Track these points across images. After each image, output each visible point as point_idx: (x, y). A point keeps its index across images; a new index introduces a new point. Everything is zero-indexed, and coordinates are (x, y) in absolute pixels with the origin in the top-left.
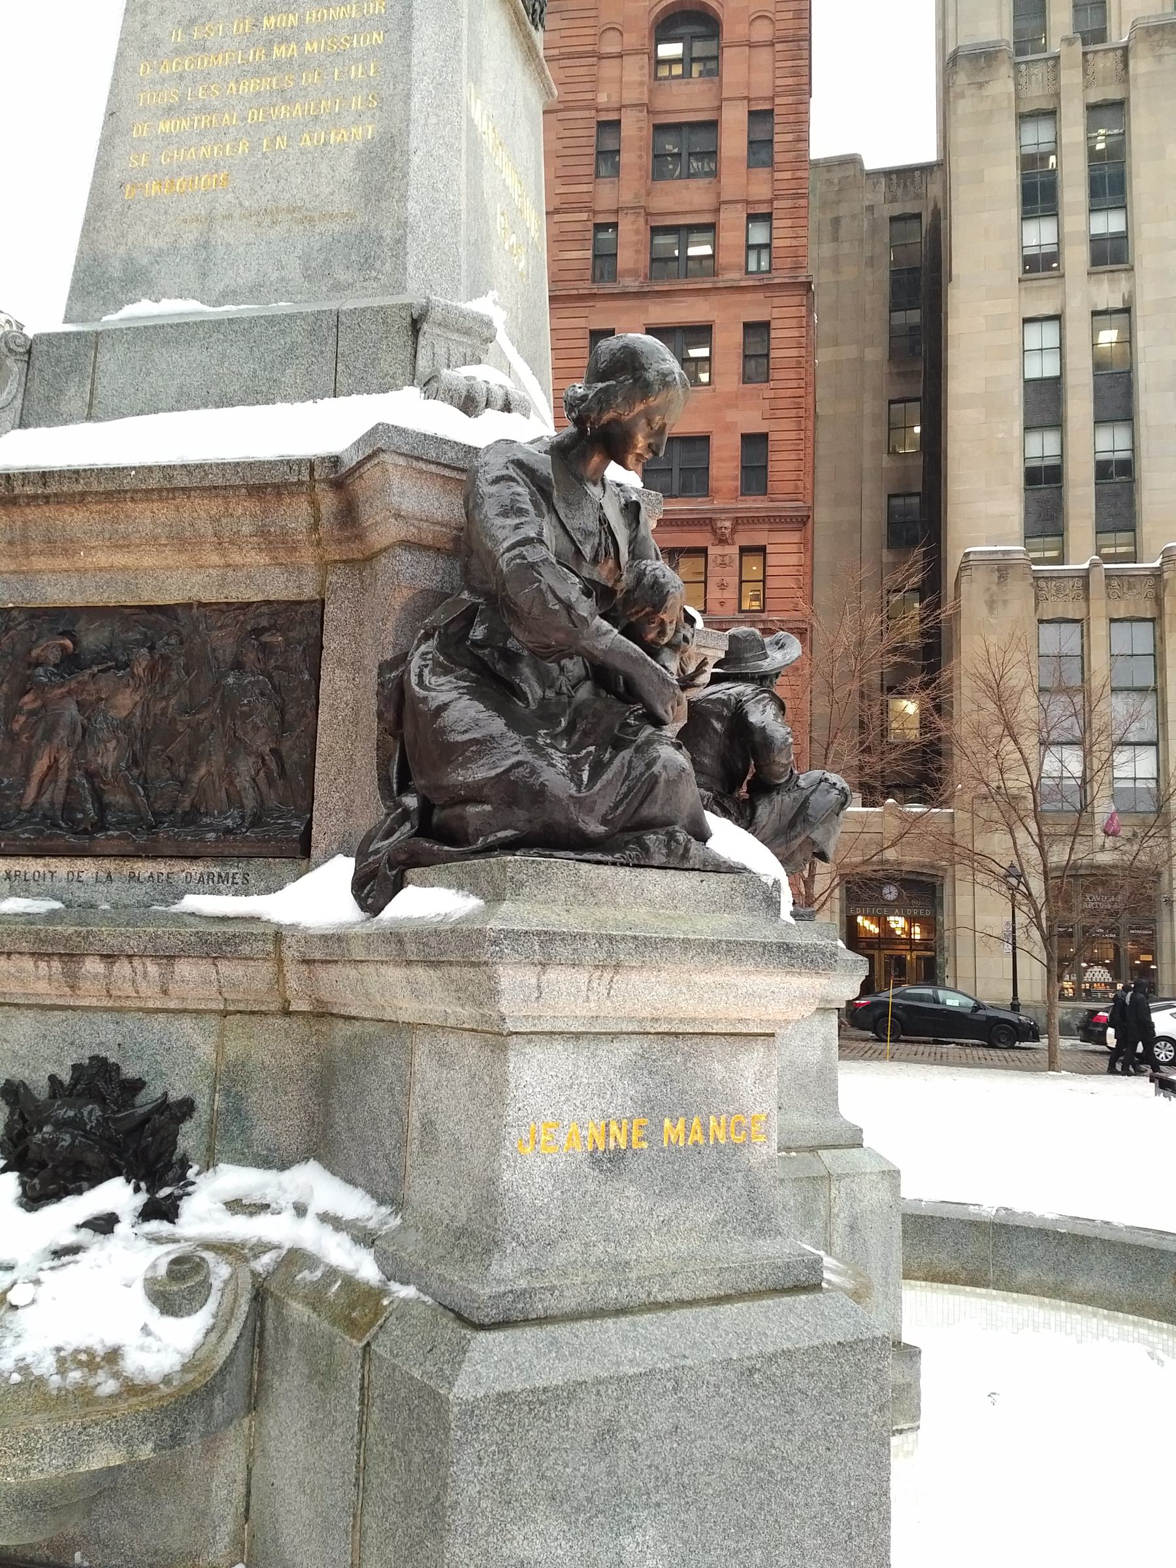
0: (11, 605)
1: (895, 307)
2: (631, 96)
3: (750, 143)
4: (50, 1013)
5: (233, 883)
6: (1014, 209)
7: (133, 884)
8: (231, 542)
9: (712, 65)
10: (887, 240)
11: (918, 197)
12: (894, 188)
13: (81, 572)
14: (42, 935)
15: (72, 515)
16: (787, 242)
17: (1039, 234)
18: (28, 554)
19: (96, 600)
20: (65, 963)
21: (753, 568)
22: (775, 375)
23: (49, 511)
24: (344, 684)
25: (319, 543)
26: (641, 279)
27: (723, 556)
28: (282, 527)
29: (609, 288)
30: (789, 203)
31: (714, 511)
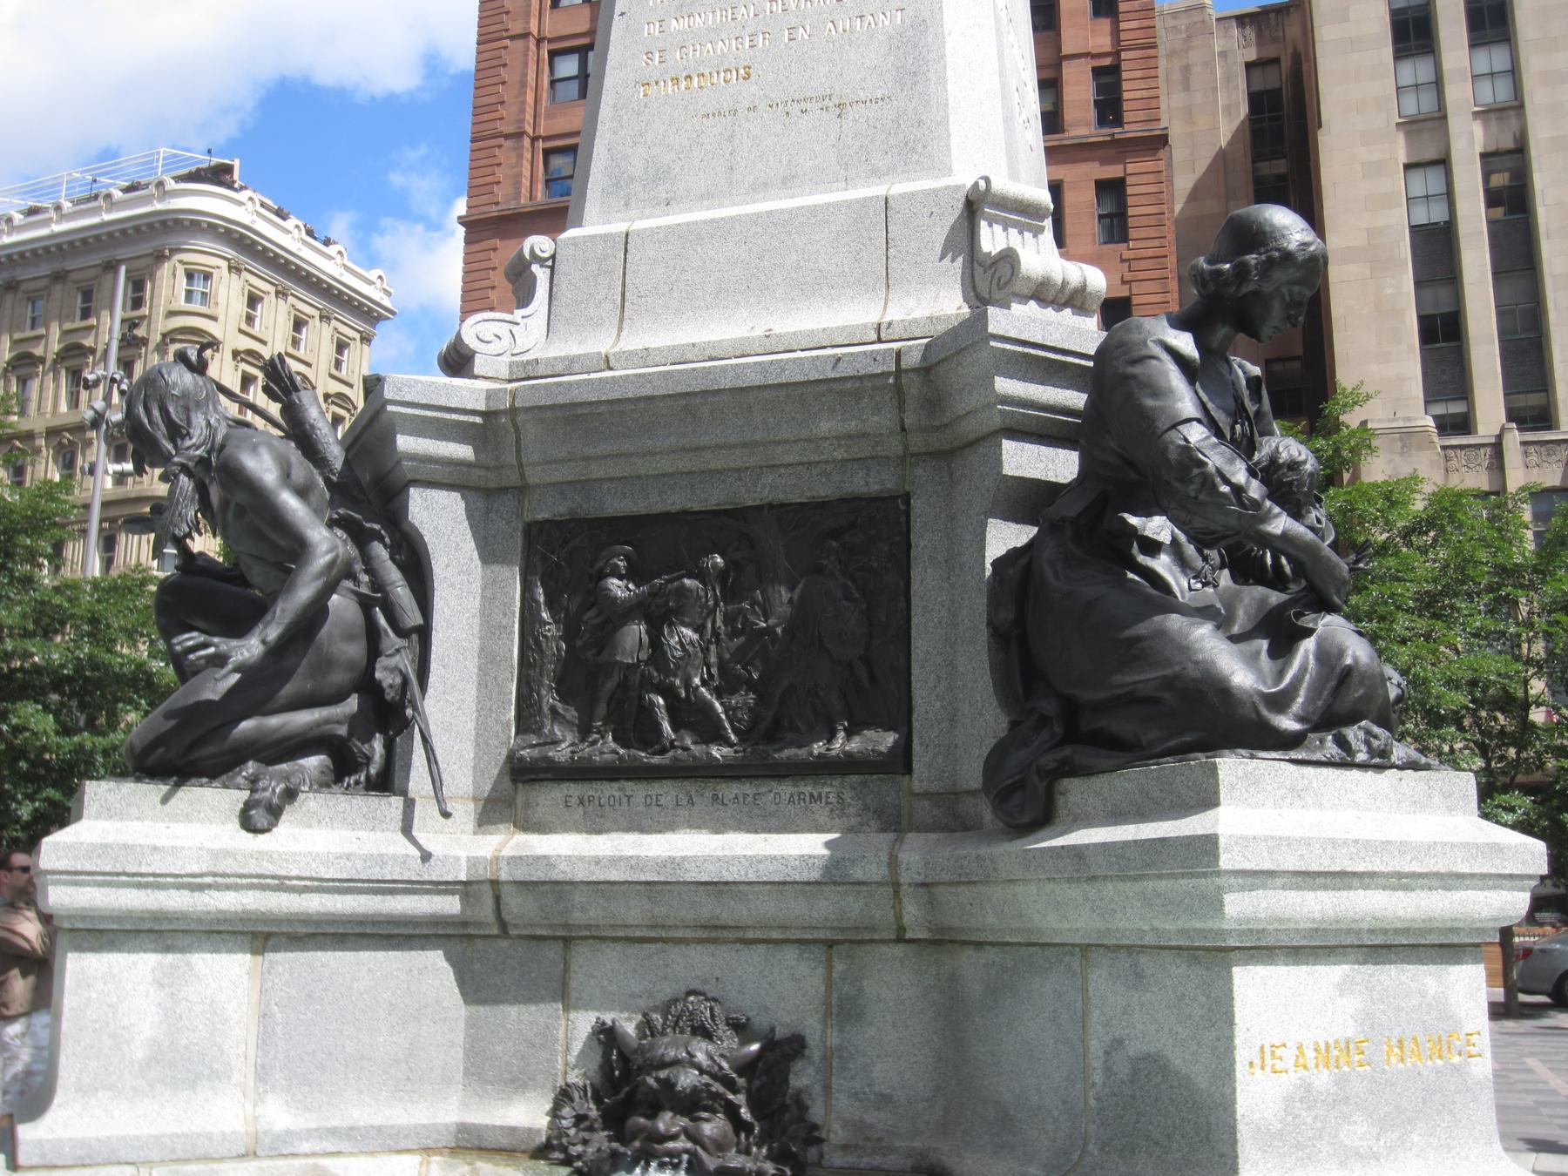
1: (1257, 157)
5: (827, 803)
6: (1388, 50)
11: (1275, 40)
22: (1133, 233)
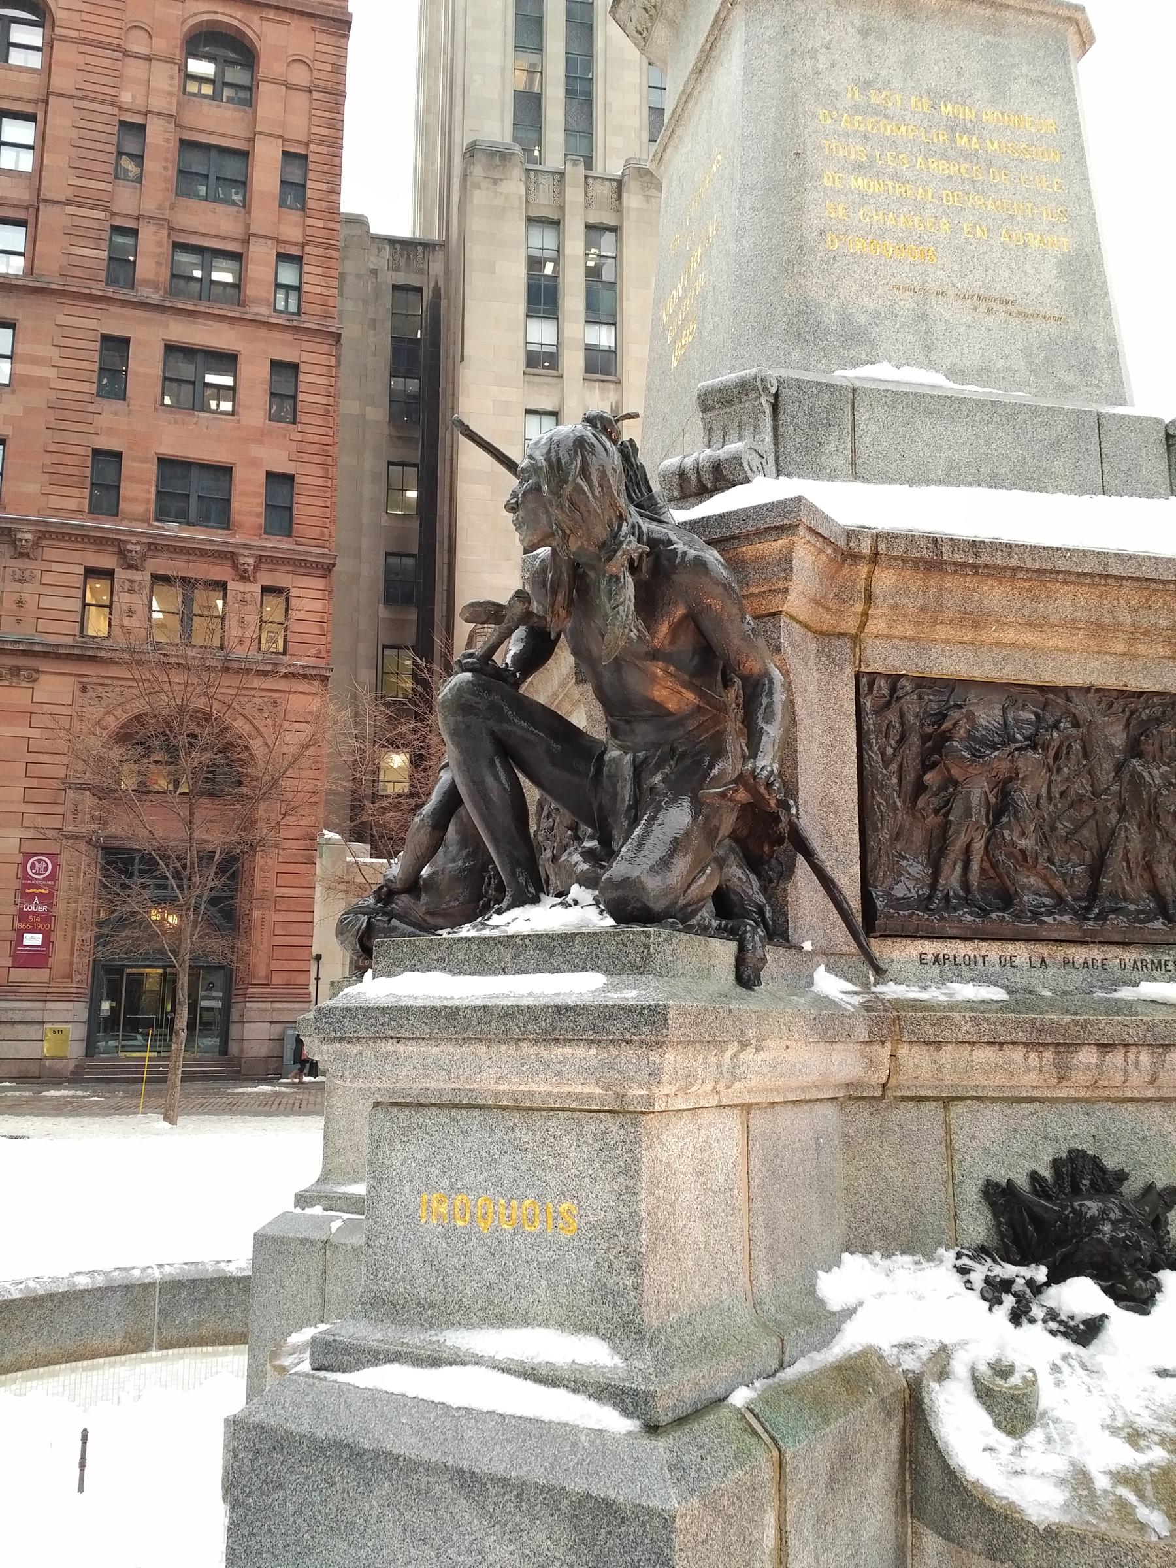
4: (1017, 1106)
6: (522, 308)
7: (1069, 969)
8: (1144, 634)
10: (389, 306)
11: (420, 271)
12: (397, 257)
14: (1038, 1024)
16: (318, 290)
17: (541, 333)
18: (935, 622)
21: (272, 608)
22: (301, 417)
23: (971, 582)
26: (162, 292)
27: (244, 593)
29: (126, 294)
31: (236, 545)
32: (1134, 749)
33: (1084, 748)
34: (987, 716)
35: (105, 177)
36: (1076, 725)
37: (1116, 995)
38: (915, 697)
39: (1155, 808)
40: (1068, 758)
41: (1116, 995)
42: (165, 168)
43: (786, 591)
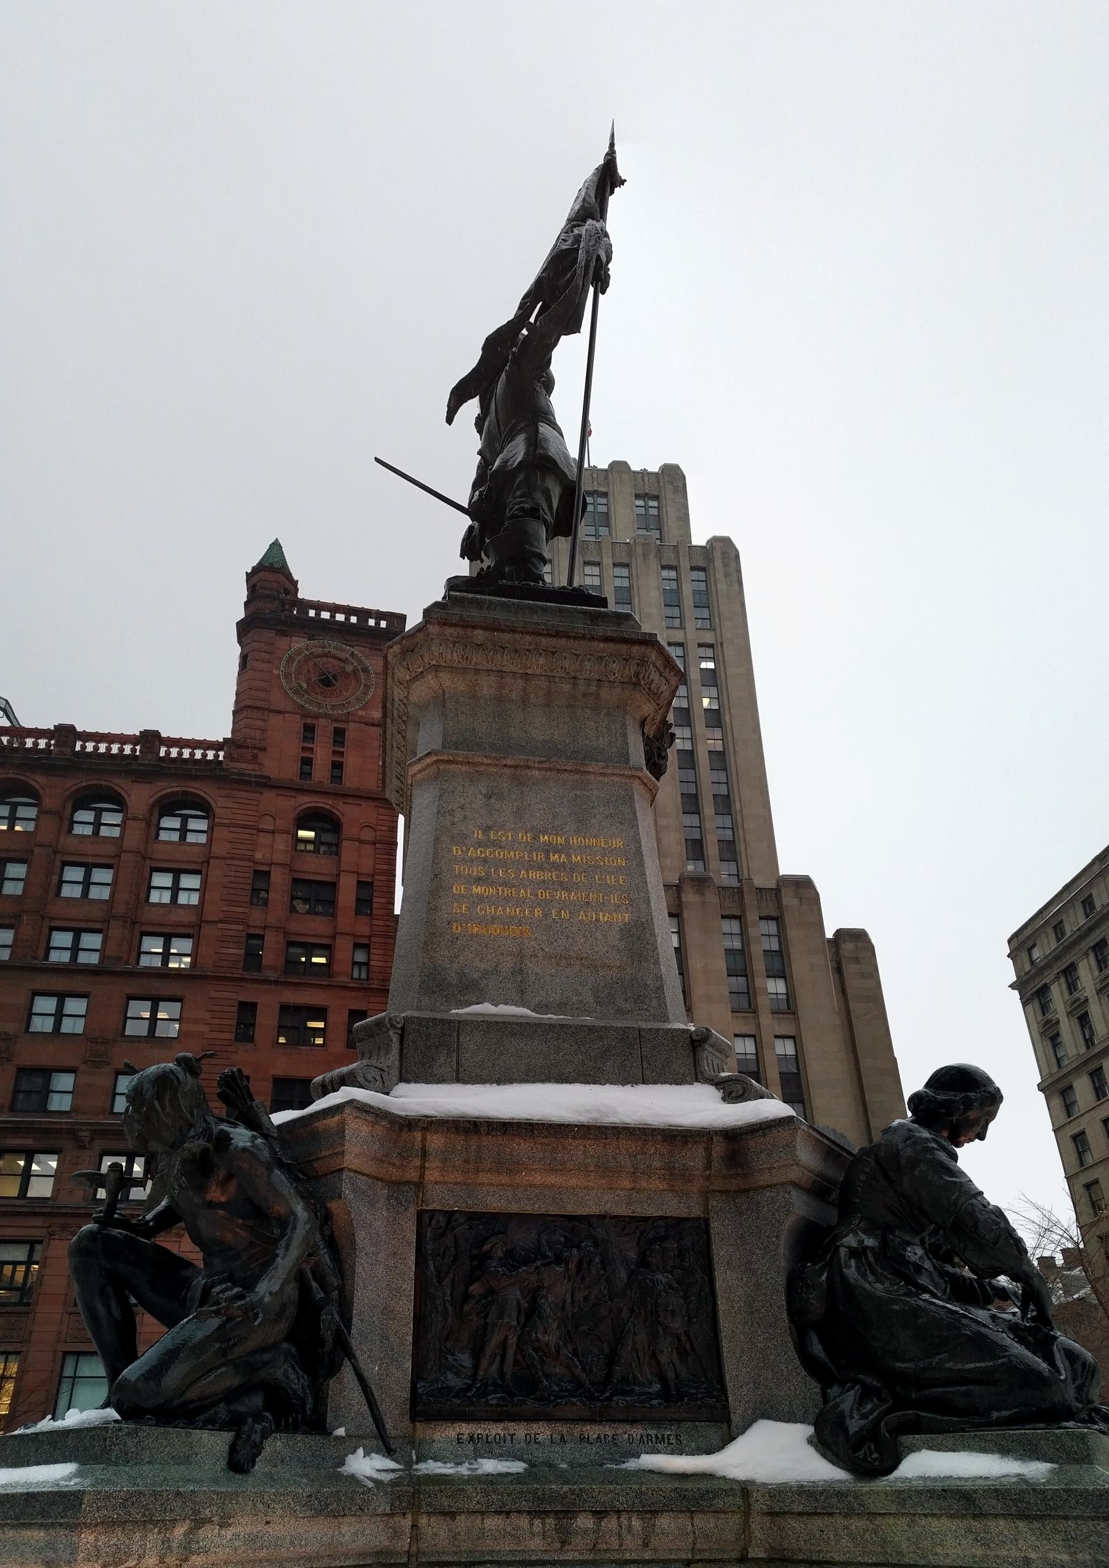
0: (456, 1209)
2: (279, 858)
3: (357, 900)
8: (642, 1173)
9: (335, 849)
13: (514, 1187)
15: (519, 1144)
16: (380, 964)
18: (477, 1171)
19: (528, 1209)
20: (559, 1519)
24: (736, 1282)
25: (709, 1177)
26: (279, 973)
28: (684, 1165)
30: (381, 940)
32: (643, 1262)
33: (602, 1261)
34: (522, 1238)
35: (243, 904)
36: (596, 1244)
37: (624, 1466)
38: (467, 1227)
39: (656, 1308)
40: (590, 1270)
41: (624, 1466)
42: (283, 897)
43: (343, 1153)
